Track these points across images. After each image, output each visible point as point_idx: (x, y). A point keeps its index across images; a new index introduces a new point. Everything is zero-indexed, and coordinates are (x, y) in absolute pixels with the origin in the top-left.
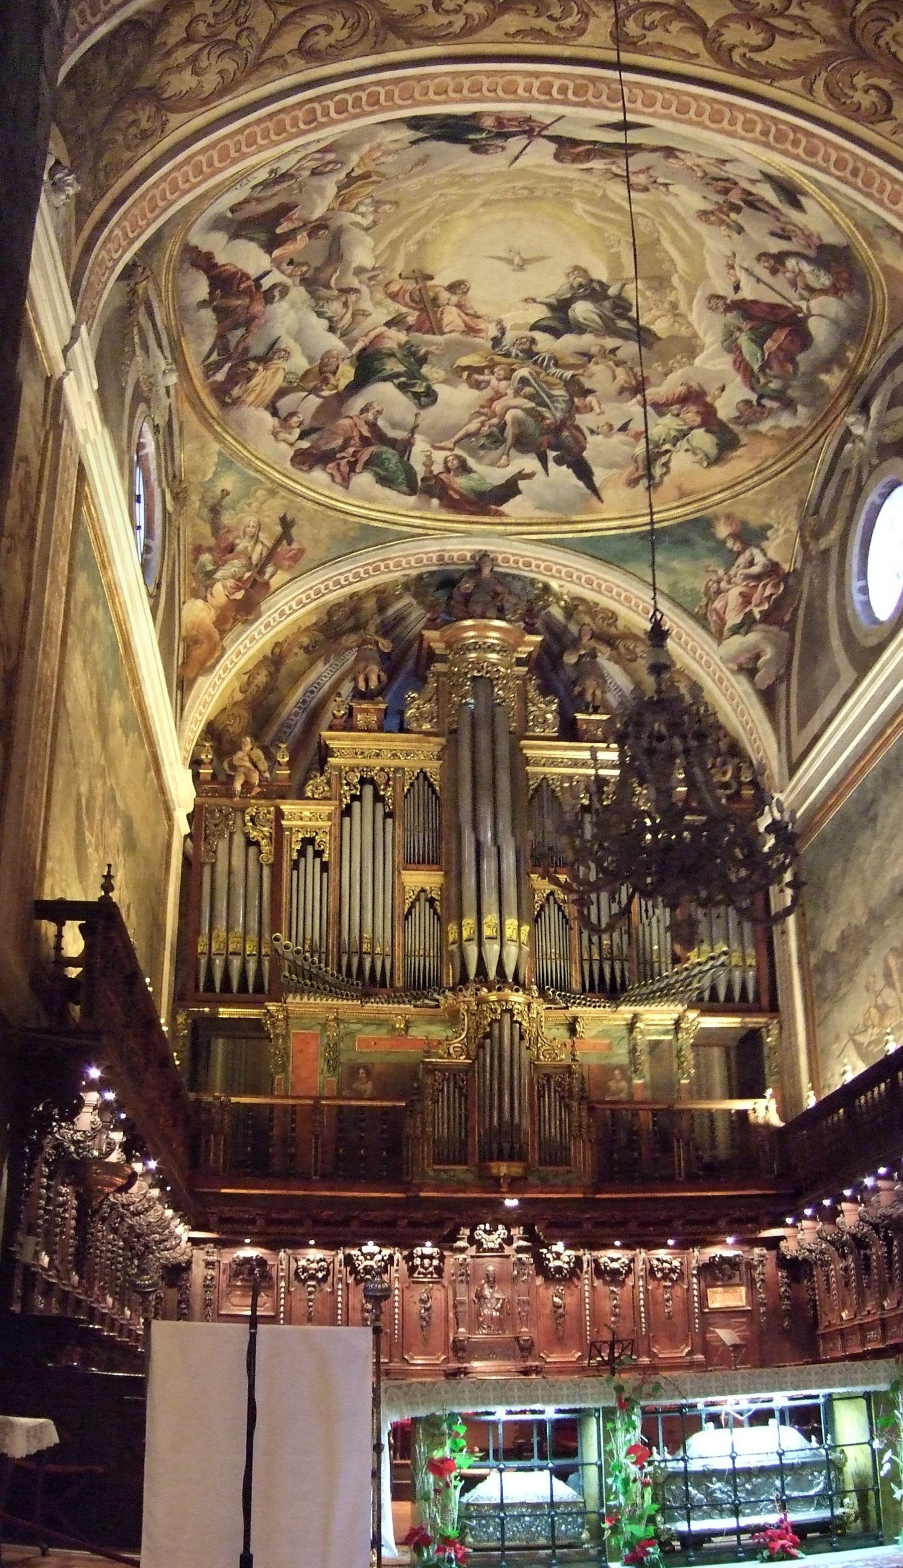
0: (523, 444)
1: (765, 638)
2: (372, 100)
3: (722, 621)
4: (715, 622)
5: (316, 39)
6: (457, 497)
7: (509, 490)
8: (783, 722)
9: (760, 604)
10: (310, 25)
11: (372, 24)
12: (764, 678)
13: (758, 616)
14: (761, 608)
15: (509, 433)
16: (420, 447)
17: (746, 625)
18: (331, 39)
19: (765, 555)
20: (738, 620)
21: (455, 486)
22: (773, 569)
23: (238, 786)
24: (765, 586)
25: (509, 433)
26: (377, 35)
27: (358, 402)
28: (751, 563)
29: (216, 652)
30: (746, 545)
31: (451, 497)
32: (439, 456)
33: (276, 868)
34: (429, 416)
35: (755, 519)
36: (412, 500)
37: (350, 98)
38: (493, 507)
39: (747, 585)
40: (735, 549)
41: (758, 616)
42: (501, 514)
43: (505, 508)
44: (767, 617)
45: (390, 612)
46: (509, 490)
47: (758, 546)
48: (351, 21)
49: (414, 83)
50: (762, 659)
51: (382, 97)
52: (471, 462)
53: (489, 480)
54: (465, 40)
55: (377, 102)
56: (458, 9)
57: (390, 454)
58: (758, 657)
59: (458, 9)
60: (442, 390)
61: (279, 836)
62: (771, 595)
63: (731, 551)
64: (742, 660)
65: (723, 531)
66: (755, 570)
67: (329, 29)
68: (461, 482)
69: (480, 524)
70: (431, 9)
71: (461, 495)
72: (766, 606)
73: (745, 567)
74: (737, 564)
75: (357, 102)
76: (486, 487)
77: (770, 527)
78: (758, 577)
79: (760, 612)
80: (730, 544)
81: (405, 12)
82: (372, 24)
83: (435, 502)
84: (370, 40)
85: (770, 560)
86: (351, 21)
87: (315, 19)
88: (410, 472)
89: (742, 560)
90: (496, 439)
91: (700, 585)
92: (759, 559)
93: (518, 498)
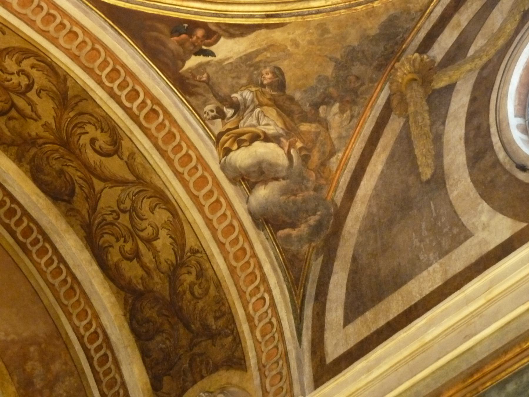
2: (114, 75)
5: (103, 146)
10: (97, 157)
11: (72, 114)
18: (98, 134)
26: (76, 104)
37: (123, 95)
48: (79, 131)
49: (83, 59)
51: (108, 69)
54: (35, 50)
55: (114, 70)
56: (22, 72)
59: (22, 72)
67: (93, 141)
70: (36, 87)
75: (121, 87)
81: (51, 101)
82: (72, 114)
84: (83, 106)
86: (79, 131)
87: (92, 157)
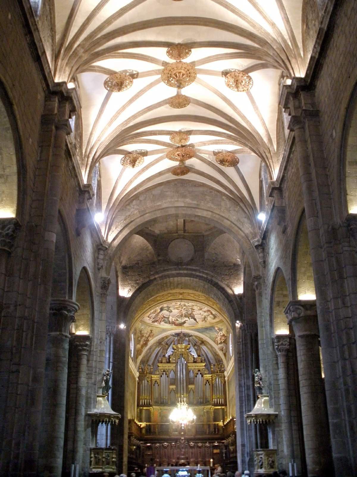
0: (186, 316)
3: (218, 342)
7: (184, 322)
12: (224, 351)
15: (183, 315)
16: (170, 318)
17: (221, 343)
22: (224, 335)
23: (145, 373)
25: (183, 315)
27: (161, 313)
29: (141, 351)
32: (173, 319)
33: (151, 385)
34: (171, 314)
35: (221, 328)
44: (224, 342)
45: (169, 338)
46: (184, 322)
52: (178, 319)
57: (166, 319)
60: (173, 311)
61: (151, 380)
65: (216, 329)
68: (177, 322)
69: (180, 327)
78: (222, 336)
88: (169, 322)
90: (182, 316)
91: (214, 336)
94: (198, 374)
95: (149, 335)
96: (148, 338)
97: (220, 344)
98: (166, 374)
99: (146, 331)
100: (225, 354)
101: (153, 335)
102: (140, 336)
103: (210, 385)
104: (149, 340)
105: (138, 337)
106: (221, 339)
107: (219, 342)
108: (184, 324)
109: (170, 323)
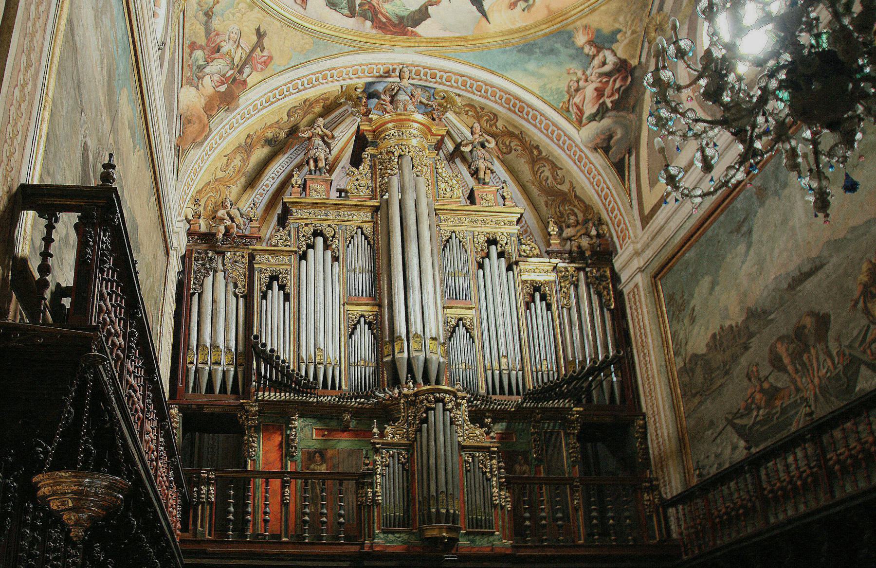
1: (616, 122)
4: (576, 113)
6: (384, 20)
8: (634, 186)
9: (612, 95)
13: (610, 105)
14: (612, 99)
19: (615, 55)
20: (594, 110)
21: (383, 11)
24: (615, 81)
28: (604, 64)
30: (599, 49)
31: (380, 21)
36: (351, 23)
38: (410, 28)
39: (601, 82)
40: (591, 53)
41: (610, 105)
42: (415, 35)
43: (419, 29)
44: (617, 105)
47: (609, 49)
50: (614, 139)
53: (407, 7)
58: (611, 137)
62: (621, 86)
63: (588, 55)
64: (598, 141)
66: (607, 68)
71: (387, 18)
72: (616, 97)
73: (599, 67)
74: (592, 65)
76: (405, 13)
77: (620, 31)
78: (608, 75)
79: (612, 102)
80: (587, 50)
83: (368, 24)
85: (619, 59)
89: (597, 61)
92: (611, 59)
93: (428, 21)
94: (488, 255)
95: (249, 56)
96: (241, 72)
97: (593, 118)
98: (327, 247)
99: (234, 27)
100: (620, 168)
101: (266, 64)
102: (202, 40)
103: (549, 307)
104: (245, 82)
105: (193, 46)
106: (600, 92)
107: (590, 109)
108: (416, 23)
109: (352, 15)
